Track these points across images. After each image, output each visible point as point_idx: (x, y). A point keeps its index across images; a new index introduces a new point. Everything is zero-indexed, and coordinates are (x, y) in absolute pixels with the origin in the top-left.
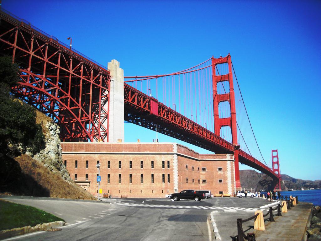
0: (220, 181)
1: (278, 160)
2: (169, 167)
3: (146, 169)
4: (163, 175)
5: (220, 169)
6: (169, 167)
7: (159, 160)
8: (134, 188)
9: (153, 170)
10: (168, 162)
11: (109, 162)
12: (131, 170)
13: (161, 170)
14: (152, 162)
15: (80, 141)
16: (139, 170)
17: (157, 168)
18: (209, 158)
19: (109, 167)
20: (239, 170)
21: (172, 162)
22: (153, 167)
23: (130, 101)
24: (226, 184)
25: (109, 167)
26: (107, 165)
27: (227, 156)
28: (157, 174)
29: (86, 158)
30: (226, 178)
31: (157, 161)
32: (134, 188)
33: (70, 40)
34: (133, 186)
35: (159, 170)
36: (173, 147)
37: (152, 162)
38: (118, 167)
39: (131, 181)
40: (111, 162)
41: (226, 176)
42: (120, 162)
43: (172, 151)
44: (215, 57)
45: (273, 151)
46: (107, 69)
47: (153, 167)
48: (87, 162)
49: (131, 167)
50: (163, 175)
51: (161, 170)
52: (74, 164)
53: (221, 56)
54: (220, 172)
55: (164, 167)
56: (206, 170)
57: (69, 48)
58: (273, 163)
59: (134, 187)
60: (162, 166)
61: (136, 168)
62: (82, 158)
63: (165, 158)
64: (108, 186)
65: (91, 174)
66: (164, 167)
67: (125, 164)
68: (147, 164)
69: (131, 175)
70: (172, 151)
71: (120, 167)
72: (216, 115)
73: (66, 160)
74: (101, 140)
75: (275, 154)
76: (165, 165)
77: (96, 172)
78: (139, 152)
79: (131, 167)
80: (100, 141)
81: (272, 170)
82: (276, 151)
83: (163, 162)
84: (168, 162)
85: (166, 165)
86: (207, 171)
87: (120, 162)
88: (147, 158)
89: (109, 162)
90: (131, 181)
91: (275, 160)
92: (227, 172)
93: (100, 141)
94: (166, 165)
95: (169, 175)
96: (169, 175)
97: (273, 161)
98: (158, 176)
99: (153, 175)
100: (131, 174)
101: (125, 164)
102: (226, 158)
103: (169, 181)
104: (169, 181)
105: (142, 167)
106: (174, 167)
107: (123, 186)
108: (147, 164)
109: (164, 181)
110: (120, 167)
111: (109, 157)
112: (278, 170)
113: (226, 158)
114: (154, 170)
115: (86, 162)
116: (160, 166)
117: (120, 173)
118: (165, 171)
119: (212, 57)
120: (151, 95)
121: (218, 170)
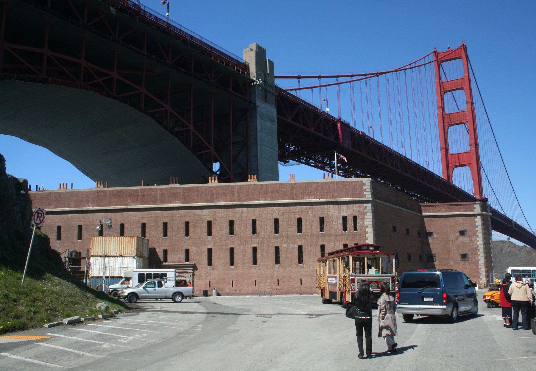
0: (464, 256)
2: (355, 229)
3: (308, 235)
5: (462, 233)
6: (355, 229)
8: (285, 274)
9: (323, 235)
10: (355, 218)
11: (232, 223)
12: (278, 237)
13: (341, 235)
14: (322, 220)
15: (173, 183)
17: (332, 232)
18: (439, 211)
19: (232, 232)
21: (362, 219)
22: (322, 229)
23: (289, 120)
24: (477, 262)
25: (232, 232)
26: (228, 230)
27: (475, 206)
28: (332, 243)
29: (185, 216)
30: (475, 251)
31: (331, 217)
32: (285, 274)
33: (166, 5)
34: (282, 270)
35: (336, 235)
36: (364, 187)
37: (322, 220)
38: (251, 231)
39: (277, 261)
40: (235, 222)
41: (476, 246)
42: (254, 222)
43: (362, 195)
44: (439, 51)
46: (243, 60)
47: (322, 229)
48: (187, 224)
49: (277, 231)
51: (341, 235)
52: (161, 229)
53: (449, 48)
54: (462, 239)
55: (345, 229)
57: (166, 20)
59: (284, 272)
60: (341, 227)
61: (289, 233)
63: (347, 211)
64: (231, 272)
66: (345, 229)
69: (277, 249)
70: (362, 195)
71: (254, 231)
72: (446, 148)
73: (144, 222)
74: (215, 180)
77: (205, 244)
78: (293, 199)
79: (277, 231)
80: (213, 181)
83: (345, 219)
84: (355, 218)
85: (350, 224)
86: (437, 238)
87: (254, 222)
88: (310, 212)
89: (232, 223)
90: (277, 261)
92: (478, 239)
93: (213, 181)
94: (350, 224)
100: (277, 245)
102: (473, 211)
105: (300, 230)
106: (367, 229)
107: (262, 270)
110: (254, 231)
111: (231, 214)
113: (473, 209)
114: (328, 235)
116: (336, 227)
117: (255, 245)
120: (328, 110)
121: (458, 234)
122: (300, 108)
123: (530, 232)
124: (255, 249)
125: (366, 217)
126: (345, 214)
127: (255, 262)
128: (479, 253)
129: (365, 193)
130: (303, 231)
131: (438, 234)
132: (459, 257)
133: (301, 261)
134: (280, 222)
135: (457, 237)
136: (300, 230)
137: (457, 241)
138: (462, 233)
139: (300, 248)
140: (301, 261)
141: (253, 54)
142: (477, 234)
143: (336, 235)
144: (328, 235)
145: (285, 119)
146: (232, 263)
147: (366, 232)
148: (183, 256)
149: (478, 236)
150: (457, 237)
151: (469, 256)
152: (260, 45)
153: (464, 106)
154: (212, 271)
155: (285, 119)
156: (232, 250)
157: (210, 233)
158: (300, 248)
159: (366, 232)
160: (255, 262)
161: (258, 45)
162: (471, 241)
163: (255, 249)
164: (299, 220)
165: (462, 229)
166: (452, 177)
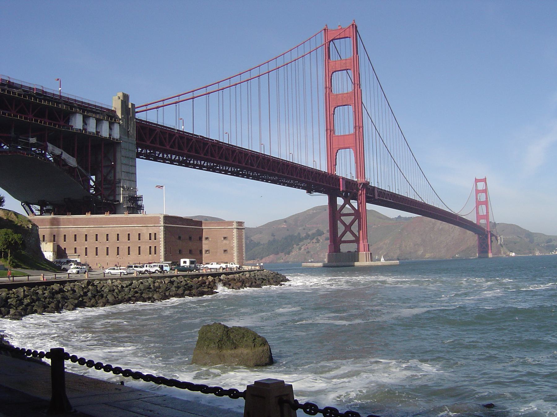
0: (225, 251)
1: (487, 198)
2: (155, 239)
4: (150, 247)
5: (225, 238)
6: (155, 239)
9: (140, 242)
10: (155, 234)
12: (118, 243)
13: (148, 242)
14: (139, 234)
16: (126, 242)
20: (348, 225)
22: (139, 239)
24: (232, 254)
28: (144, 246)
30: (232, 248)
36: (160, 219)
41: (232, 246)
42: (107, 235)
44: (329, 28)
45: (477, 181)
47: (139, 239)
50: (150, 247)
51: (148, 242)
53: (339, 26)
54: (225, 241)
55: (150, 239)
56: (210, 239)
58: (479, 203)
61: (124, 241)
62: (71, 232)
63: (152, 231)
64: (96, 258)
65: (80, 247)
66: (150, 239)
67: (113, 238)
68: (134, 237)
75: (481, 186)
76: (152, 238)
82: (484, 180)
83: (150, 234)
84: (155, 234)
85: (153, 237)
91: (482, 197)
92: (234, 242)
94: (153, 237)
95: (155, 247)
96: (155, 247)
97: (477, 199)
98: (145, 248)
99: (139, 247)
101: (113, 238)
103: (155, 254)
105: (129, 240)
108: (134, 237)
109: (150, 254)
112: (486, 217)
115: (74, 236)
117: (108, 246)
118: (152, 243)
119: (324, 27)
121: (223, 239)
122: (157, 132)
123: (447, 210)
124: (108, 248)
125: (160, 234)
127: (107, 254)
128: (234, 249)
129: (161, 222)
130: (130, 240)
132: (223, 251)
133: (129, 254)
134: (119, 235)
135: (222, 240)
136: (129, 240)
137: (222, 242)
138: (225, 238)
139: (129, 247)
140: (129, 254)
141: (120, 102)
142: (234, 239)
145: (145, 143)
146: (97, 255)
148: (74, 251)
149: (234, 240)
150: (222, 240)
151: (229, 251)
152: (125, 93)
153: (349, 88)
154: (87, 258)
155: (145, 143)
156: (97, 248)
157: (86, 240)
158: (129, 247)
160: (107, 254)
161: (124, 94)
162: (230, 243)
163: (108, 248)
164: (129, 234)
166: (336, 159)
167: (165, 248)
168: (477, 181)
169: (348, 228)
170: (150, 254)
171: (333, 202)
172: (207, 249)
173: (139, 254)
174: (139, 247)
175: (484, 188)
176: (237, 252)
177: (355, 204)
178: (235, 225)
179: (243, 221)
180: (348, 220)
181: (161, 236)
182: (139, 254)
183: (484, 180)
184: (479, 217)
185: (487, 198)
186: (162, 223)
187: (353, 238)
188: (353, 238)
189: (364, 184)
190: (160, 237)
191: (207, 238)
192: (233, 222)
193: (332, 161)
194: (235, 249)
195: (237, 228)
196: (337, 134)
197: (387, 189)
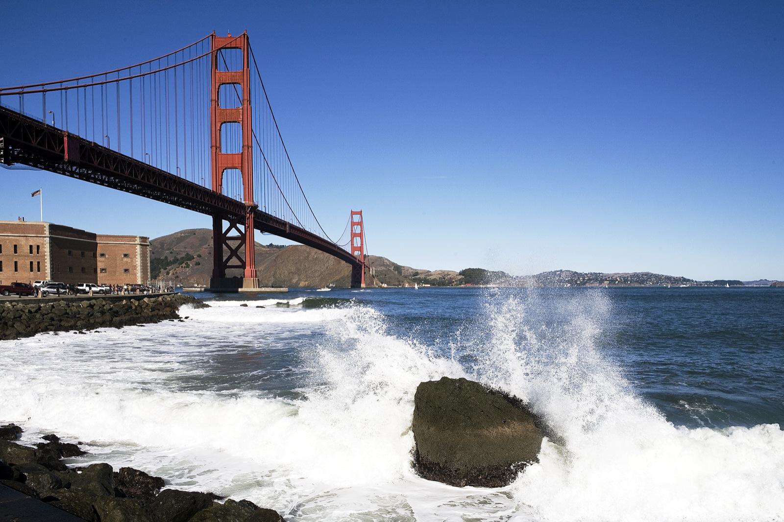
0: (126, 270)
1: (362, 230)
4: (31, 263)
5: (126, 255)
7: (24, 244)
10: (38, 247)
13: (28, 256)
14: (15, 246)
22: (16, 252)
24: (135, 274)
30: (135, 267)
35: (25, 256)
37: (15, 246)
43: (43, 233)
45: (353, 213)
47: (16, 252)
51: (28, 256)
54: (125, 259)
55: (31, 252)
56: (107, 256)
58: (354, 235)
63: (33, 242)
66: (31, 252)
70: (43, 233)
75: (356, 218)
76: (33, 251)
81: (348, 249)
82: (360, 213)
83: (31, 247)
84: (38, 247)
85: (35, 250)
91: (357, 230)
94: (35, 250)
95: (39, 263)
96: (39, 263)
97: (352, 231)
98: (24, 263)
103: (39, 270)
104: (39, 270)
109: (32, 270)
112: (361, 249)
114: (18, 256)
121: (123, 256)
126: (31, 244)
131: (109, 255)
137: (122, 260)
138: (126, 255)
143: (25, 256)
144: (18, 256)
147: (45, 255)
151: (130, 270)
159: (45, 255)
162: (132, 261)
165: (125, 253)
166: (222, 178)
167: (52, 264)
168: (353, 213)
169: (234, 253)
170: (32, 270)
171: (217, 225)
172: (103, 267)
173: (16, 270)
174: (16, 262)
175: (360, 221)
176: (141, 272)
177: (242, 227)
178: (138, 241)
179: (148, 236)
180: (234, 244)
181: (47, 249)
182: (16, 270)
183: (360, 213)
184: (354, 249)
185: (362, 230)
186: (47, 233)
187: (239, 264)
188: (239, 264)
189: (252, 207)
190: (45, 250)
191: (102, 255)
192: (135, 237)
193: (218, 178)
194: (139, 268)
195: (140, 245)
196: (224, 151)
197: (273, 215)
